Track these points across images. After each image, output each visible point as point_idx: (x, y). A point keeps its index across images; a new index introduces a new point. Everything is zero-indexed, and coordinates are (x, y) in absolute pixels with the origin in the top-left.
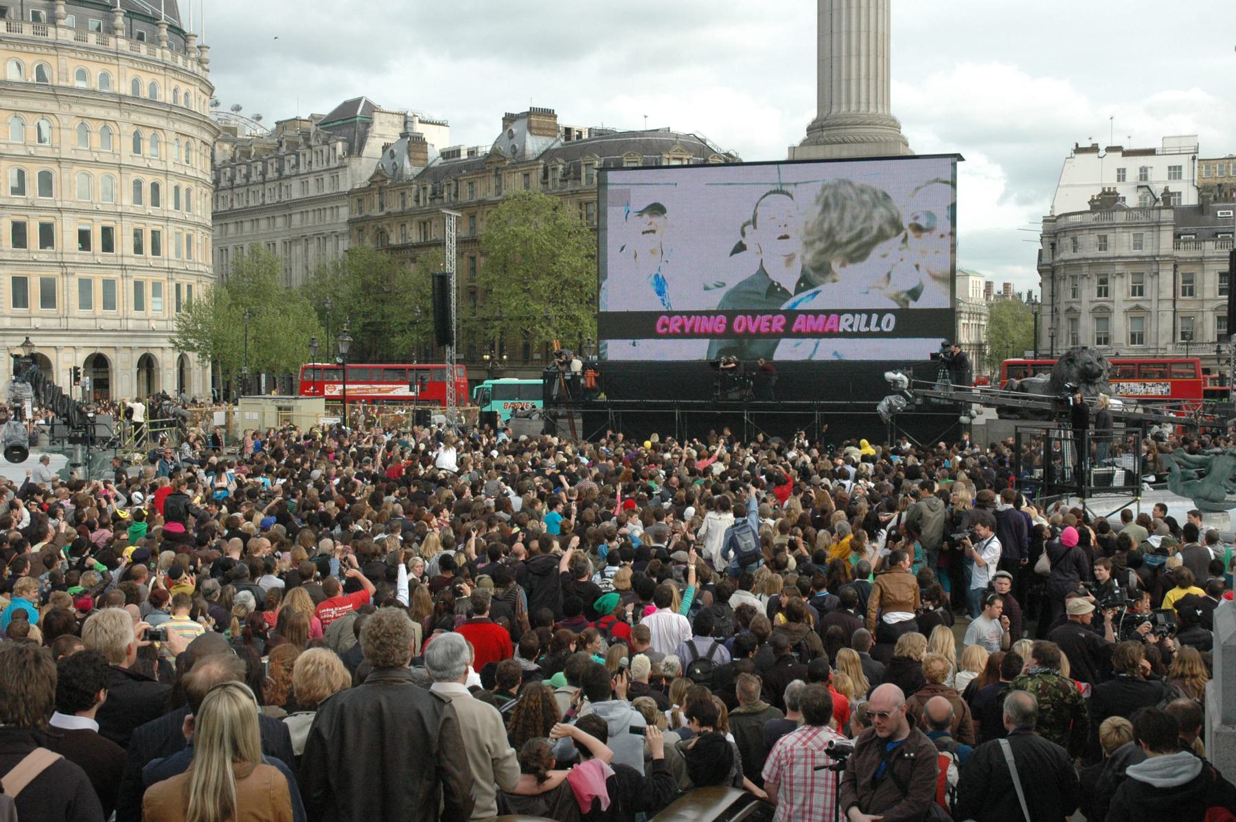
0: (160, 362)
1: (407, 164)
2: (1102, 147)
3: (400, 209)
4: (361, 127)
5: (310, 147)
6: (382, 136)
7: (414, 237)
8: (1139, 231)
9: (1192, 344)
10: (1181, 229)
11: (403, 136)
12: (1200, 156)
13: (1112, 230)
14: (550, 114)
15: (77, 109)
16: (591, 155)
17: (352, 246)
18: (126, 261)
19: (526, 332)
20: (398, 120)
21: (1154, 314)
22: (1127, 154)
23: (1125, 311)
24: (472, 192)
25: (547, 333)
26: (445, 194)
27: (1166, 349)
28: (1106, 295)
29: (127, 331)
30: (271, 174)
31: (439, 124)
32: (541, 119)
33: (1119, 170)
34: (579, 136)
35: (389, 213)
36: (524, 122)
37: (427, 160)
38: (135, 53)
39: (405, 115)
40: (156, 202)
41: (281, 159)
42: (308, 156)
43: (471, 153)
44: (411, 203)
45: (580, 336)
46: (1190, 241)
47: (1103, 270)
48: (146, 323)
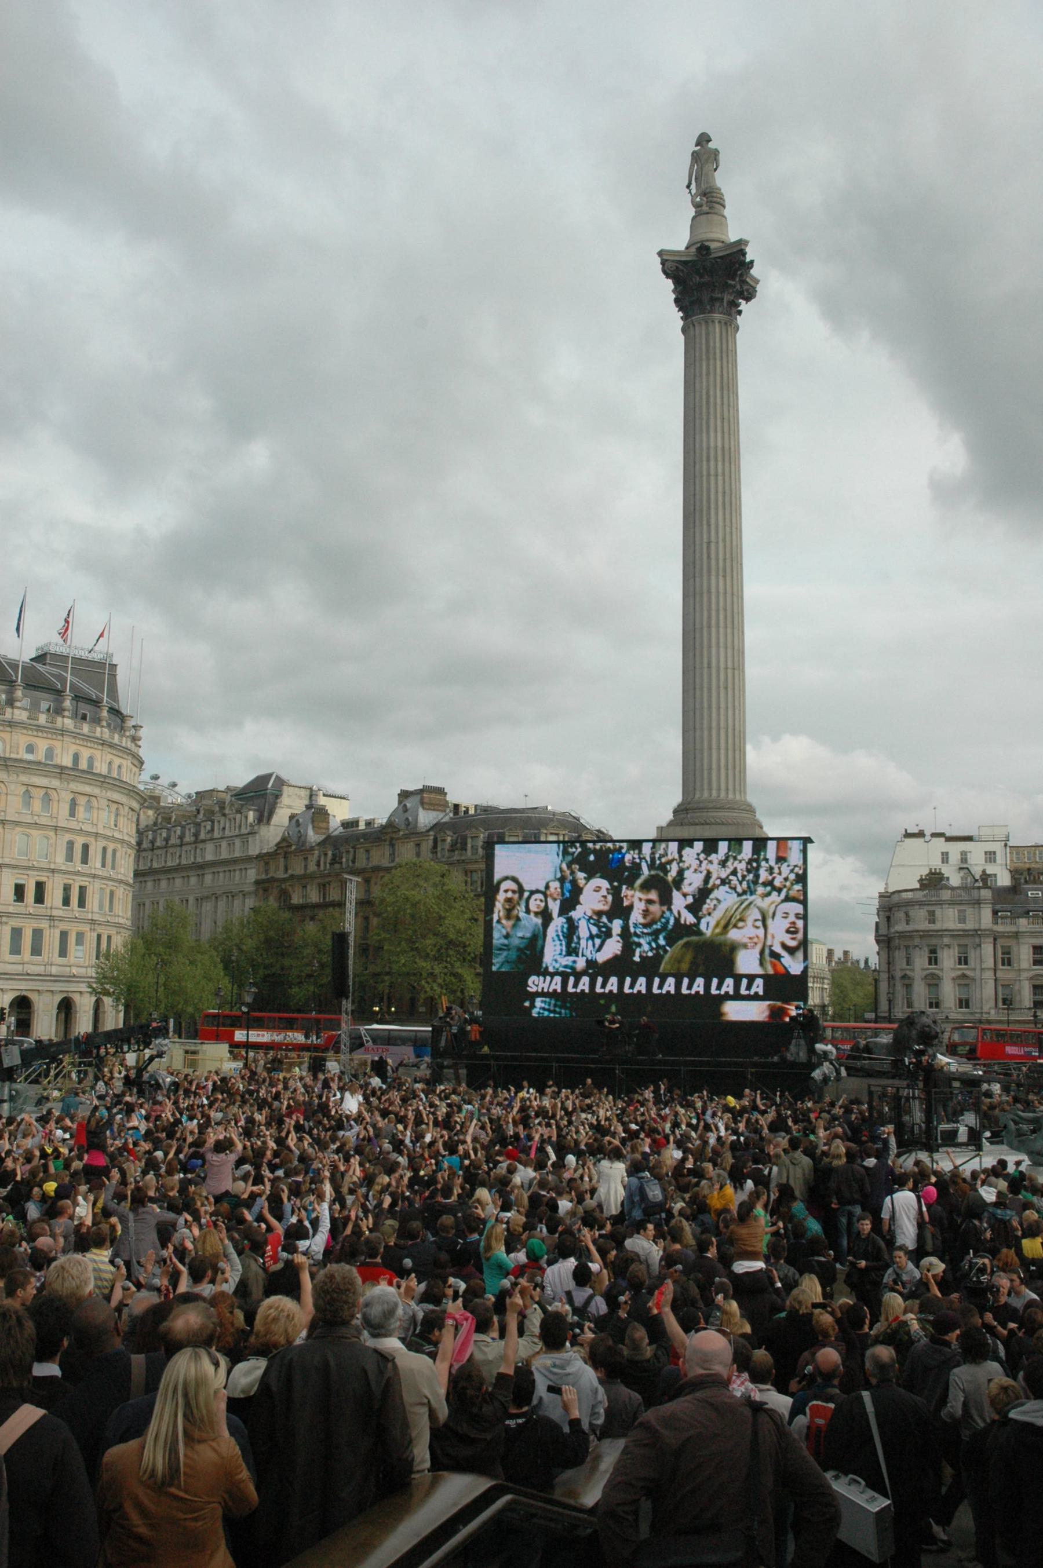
0: (78, 1004)
1: (311, 832)
2: (928, 833)
3: (302, 872)
4: (271, 798)
5: (224, 815)
6: (289, 807)
7: (314, 897)
8: (962, 907)
9: (1013, 1009)
10: (998, 907)
11: (309, 807)
12: (1010, 844)
14: (441, 791)
15: (24, 778)
16: (477, 829)
17: (257, 904)
18: (55, 913)
19: (414, 987)
20: (305, 793)
21: (978, 982)
22: (949, 839)
23: (953, 979)
24: (368, 859)
25: (432, 989)
26: (344, 860)
28: (936, 964)
29: (51, 975)
30: (189, 838)
31: (341, 798)
32: (433, 796)
33: (943, 853)
34: (467, 811)
35: (292, 876)
36: (417, 798)
37: (328, 829)
38: (78, 731)
39: (311, 789)
40: (85, 860)
41: (198, 825)
42: (222, 822)
43: (369, 823)
44: (312, 867)
45: (462, 991)
46: (1006, 917)
47: (934, 941)
48: (68, 969)
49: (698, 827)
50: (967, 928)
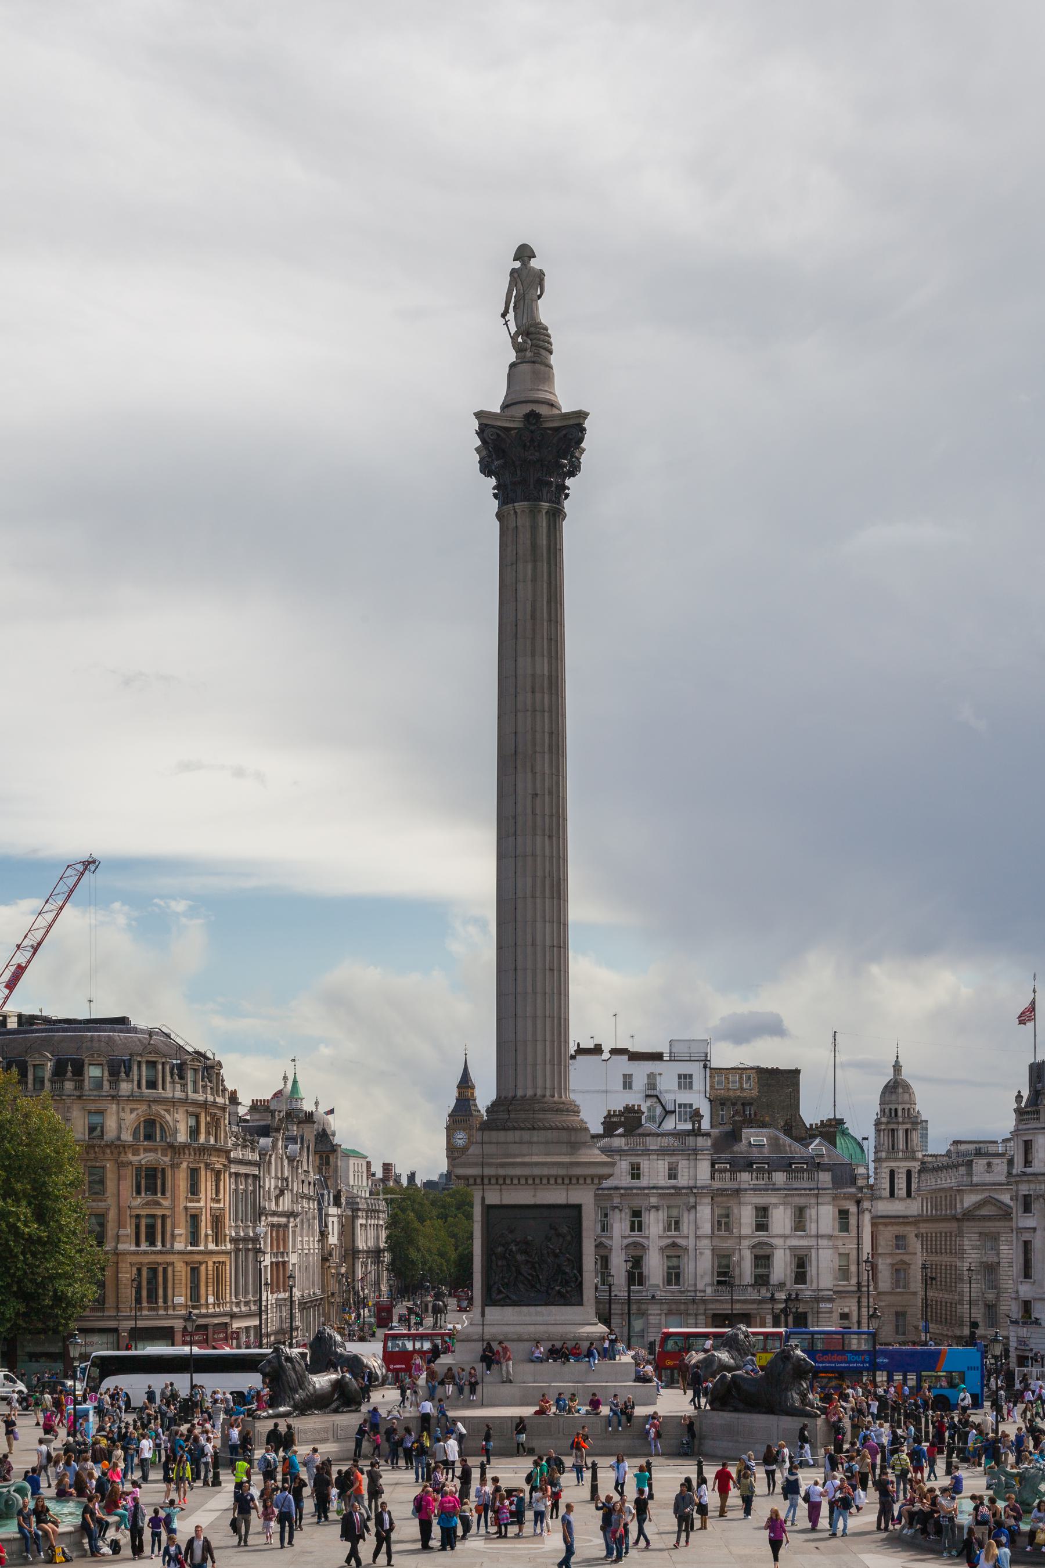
2: (606, 1048)
8: (674, 1159)
13: (647, 1158)
21: (692, 1253)
23: (662, 1249)
27: (704, 1291)
28: (640, 1230)
33: (625, 1075)
46: (725, 1171)
49: (523, 1132)
50: (680, 1185)
